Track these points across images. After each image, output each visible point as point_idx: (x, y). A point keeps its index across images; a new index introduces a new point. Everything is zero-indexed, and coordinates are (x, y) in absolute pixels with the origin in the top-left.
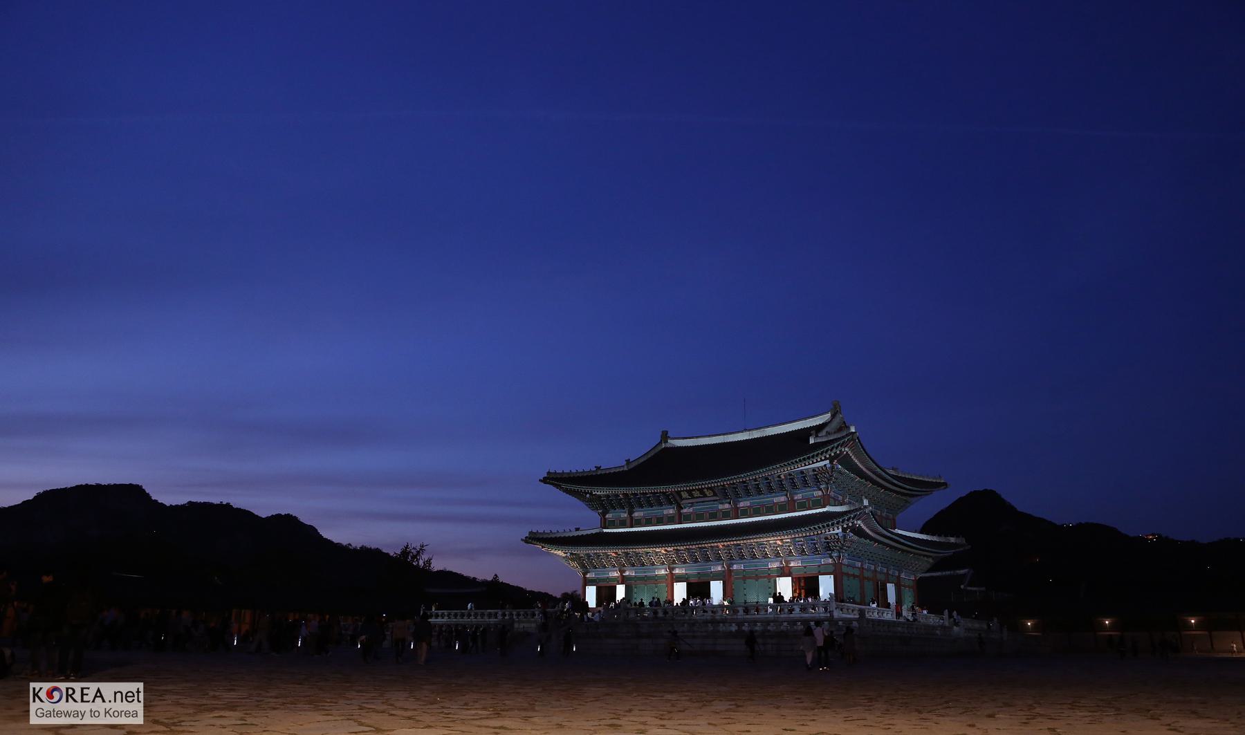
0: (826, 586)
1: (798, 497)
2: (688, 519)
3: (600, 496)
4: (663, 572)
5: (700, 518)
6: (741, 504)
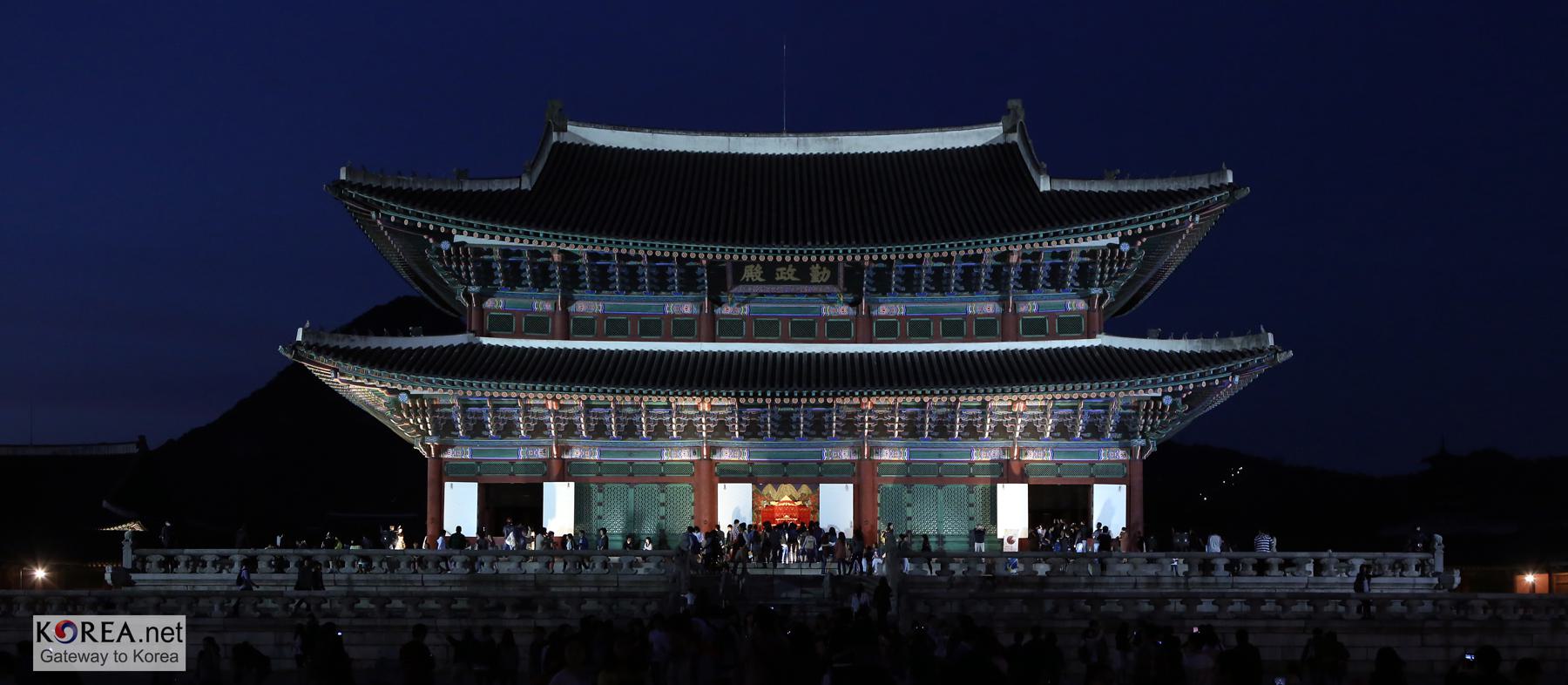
0: (1110, 507)
1: (1029, 307)
2: (732, 330)
3: (478, 250)
4: (685, 455)
5: (766, 331)
6: (883, 310)
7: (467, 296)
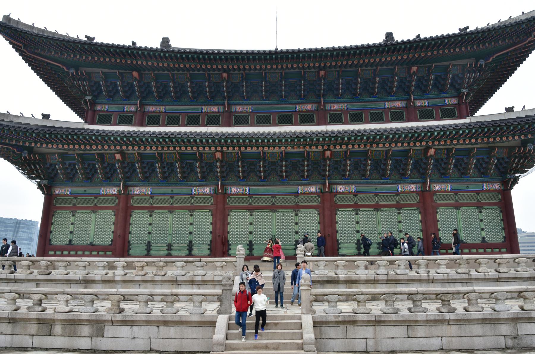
7: (85, 102)
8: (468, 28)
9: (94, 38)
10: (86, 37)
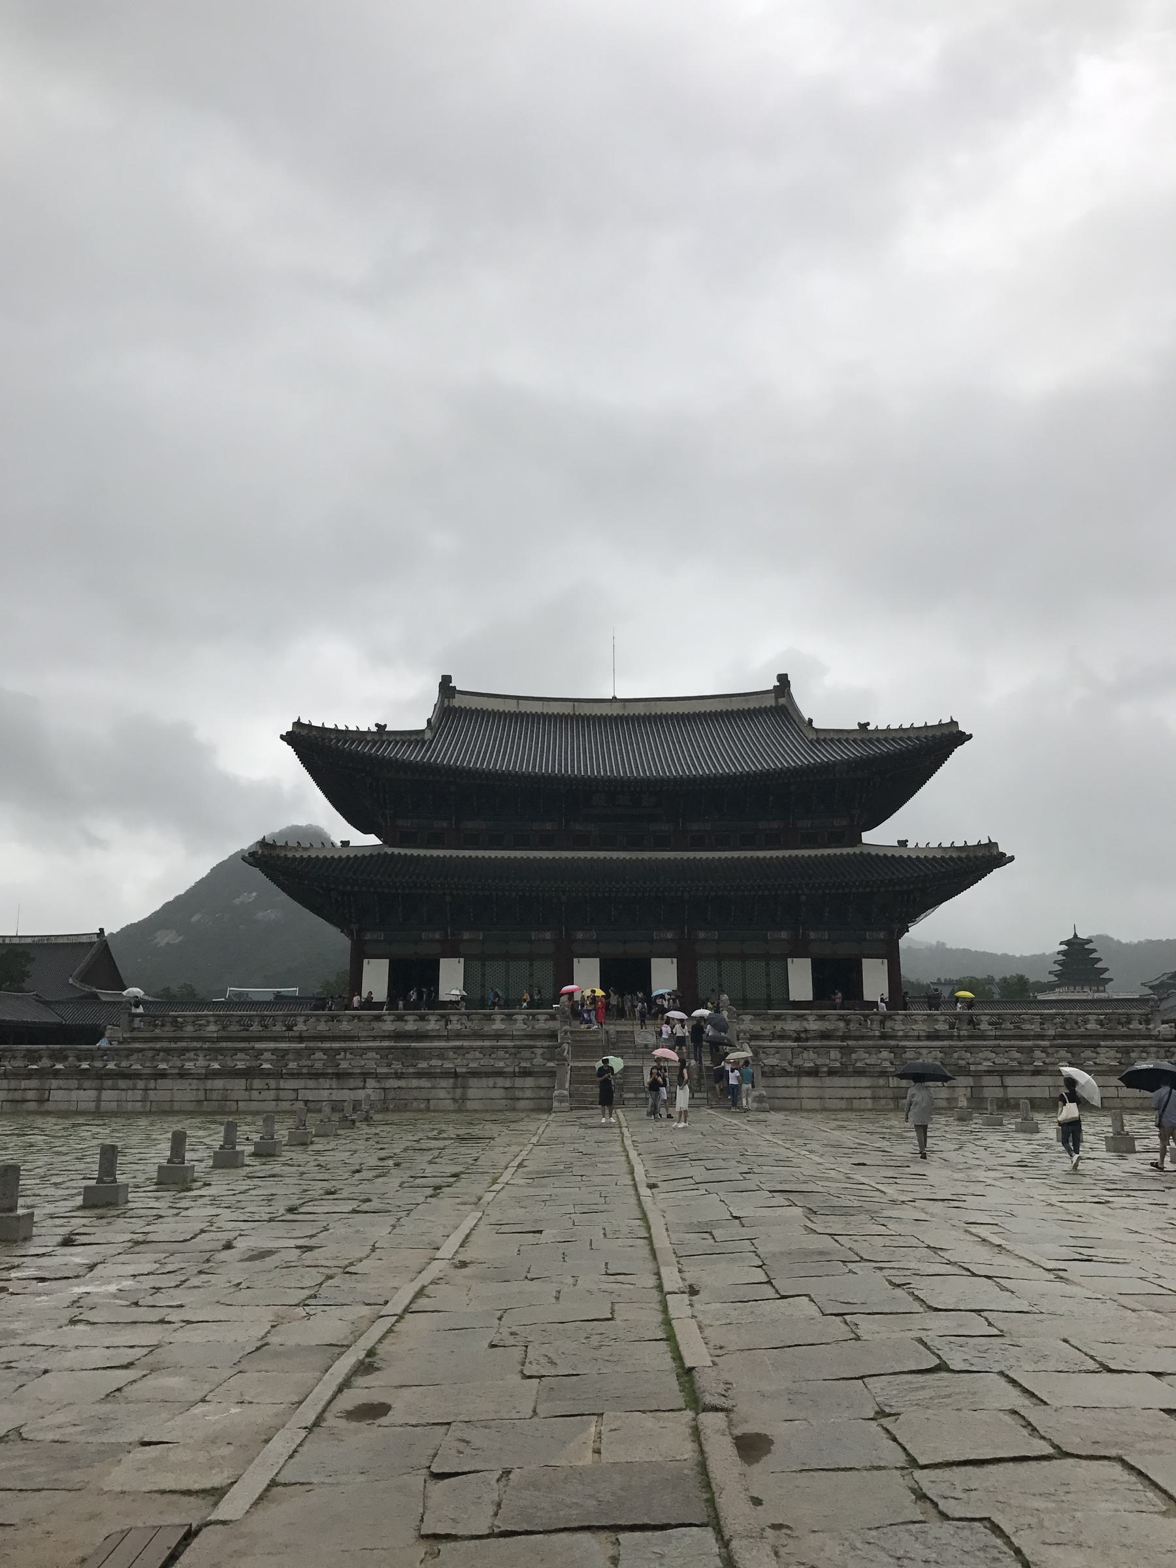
8: (868, 724)
9: (385, 726)
10: (377, 725)
